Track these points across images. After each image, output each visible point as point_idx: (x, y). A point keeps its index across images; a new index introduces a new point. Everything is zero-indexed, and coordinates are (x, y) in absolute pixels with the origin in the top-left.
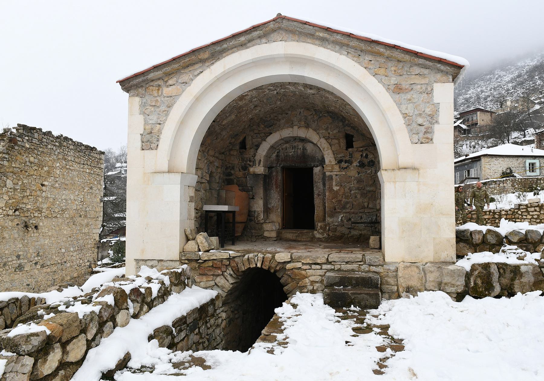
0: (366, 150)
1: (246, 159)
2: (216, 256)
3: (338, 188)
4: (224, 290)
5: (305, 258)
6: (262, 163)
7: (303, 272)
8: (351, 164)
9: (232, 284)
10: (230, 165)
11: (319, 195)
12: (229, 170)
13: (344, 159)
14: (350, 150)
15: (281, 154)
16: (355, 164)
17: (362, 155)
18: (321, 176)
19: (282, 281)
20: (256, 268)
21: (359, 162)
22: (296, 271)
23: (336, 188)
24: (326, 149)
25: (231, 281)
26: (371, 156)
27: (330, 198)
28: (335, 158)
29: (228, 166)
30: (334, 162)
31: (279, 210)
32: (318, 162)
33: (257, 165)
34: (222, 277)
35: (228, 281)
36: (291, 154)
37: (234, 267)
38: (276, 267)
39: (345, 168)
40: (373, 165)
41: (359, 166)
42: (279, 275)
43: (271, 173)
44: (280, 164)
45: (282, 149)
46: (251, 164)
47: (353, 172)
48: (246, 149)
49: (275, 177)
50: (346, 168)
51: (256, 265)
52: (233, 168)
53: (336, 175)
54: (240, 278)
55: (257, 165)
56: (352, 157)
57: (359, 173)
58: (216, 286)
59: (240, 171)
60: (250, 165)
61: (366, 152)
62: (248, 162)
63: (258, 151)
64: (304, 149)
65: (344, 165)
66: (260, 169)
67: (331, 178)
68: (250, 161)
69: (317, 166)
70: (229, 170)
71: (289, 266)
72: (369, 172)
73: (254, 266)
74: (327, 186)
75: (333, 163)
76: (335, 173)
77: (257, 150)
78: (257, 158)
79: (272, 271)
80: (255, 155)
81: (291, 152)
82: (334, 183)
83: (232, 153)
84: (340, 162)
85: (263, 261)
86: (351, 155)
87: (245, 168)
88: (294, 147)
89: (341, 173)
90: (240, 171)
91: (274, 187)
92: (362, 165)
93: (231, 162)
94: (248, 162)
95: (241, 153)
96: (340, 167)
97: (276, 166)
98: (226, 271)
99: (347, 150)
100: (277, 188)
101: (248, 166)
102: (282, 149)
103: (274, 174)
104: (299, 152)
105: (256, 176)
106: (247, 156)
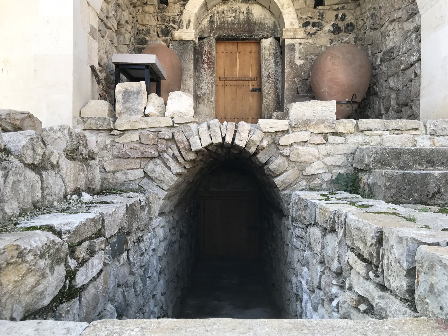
0: (343, 8)
1: (167, 19)
2: (147, 123)
3: (302, 62)
4: (163, 185)
5: (316, 124)
6: (192, 25)
7: (313, 150)
8: (321, 29)
9: (178, 174)
10: (144, 28)
11: (269, 78)
12: (142, 36)
13: (311, 21)
14: (320, 8)
15: (216, 19)
16: (328, 27)
17: (337, 16)
18: (273, 51)
19: (272, 166)
20: (222, 145)
21: (333, 25)
22: (301, 149)
23: (299, 62)
24: (286, 6)
25: (176, 169)
26: (349, 18)
27: (291, 76)
28: (299, 19)
29: (141, 28)
30: (297, 25)
31: (213, 99)
32: (268, 32)
33: (185, 27)
34: (158, 161)
35: (169, 168)
36: (230, 19)
37: (182, 142)
38: (261, 141)
39: (312, 34)
40: (352, 30)
41: (333, 32)
42: (262, 157)
43: (202, 46)
44: (215, 34)
45: (218, 12)
46: (176, 26)
47: (323, 38)
48: (167, 4)
49: (207, 52)
50: (314, 33)
51: (224, 138)
52: (148, 32)
53: (300, 44)
54: (188, 167)
55: (185, 27)
56: (322, 19)
57: (332, 41)
58: (146, 180)
59: (159, 36)
60: (174, 29)
61: (343, 11)
62: (171, 24)
63: (186, 7)
64: (249, 13)
65: (311, 29)
66: (188, 34)
67: (292, 47)
68: (174, 22)
69: (267, 38)
70: (142, 36)
71: (283, 140)
72: (346, 39)
73: (220, 140)
74: (287, 60)
75: (295, 27)
76: (299, 41)
77: (184, 5)
78: (185, 17)
79: (253, 150)
80: (181, 14)
81: (230, 17)
82: (297, 55)
83: (147, 8)
84: (305, 25)
85: (236, 131)
86: (321, 15)
87: (166, 32)
88: (234, 10)
89: (307, 41)
90: (159, 36)
91: (206, 66)
92: (336, 30)
93: (145, 23)
94: (171, 24)
95: (161, 10)
96: (305, 32)
97: (209, 36)
98: (165, 151)
99: (315, 8)
100: (209, 67)
101: (170, 29)
102: (218, 12)
103: (206, 47)
104: (242, 16)
105: (183, 43)
106: (170, 14)
